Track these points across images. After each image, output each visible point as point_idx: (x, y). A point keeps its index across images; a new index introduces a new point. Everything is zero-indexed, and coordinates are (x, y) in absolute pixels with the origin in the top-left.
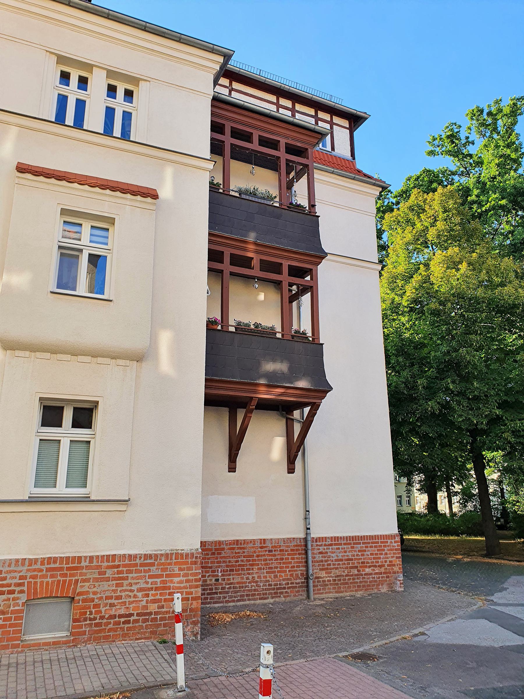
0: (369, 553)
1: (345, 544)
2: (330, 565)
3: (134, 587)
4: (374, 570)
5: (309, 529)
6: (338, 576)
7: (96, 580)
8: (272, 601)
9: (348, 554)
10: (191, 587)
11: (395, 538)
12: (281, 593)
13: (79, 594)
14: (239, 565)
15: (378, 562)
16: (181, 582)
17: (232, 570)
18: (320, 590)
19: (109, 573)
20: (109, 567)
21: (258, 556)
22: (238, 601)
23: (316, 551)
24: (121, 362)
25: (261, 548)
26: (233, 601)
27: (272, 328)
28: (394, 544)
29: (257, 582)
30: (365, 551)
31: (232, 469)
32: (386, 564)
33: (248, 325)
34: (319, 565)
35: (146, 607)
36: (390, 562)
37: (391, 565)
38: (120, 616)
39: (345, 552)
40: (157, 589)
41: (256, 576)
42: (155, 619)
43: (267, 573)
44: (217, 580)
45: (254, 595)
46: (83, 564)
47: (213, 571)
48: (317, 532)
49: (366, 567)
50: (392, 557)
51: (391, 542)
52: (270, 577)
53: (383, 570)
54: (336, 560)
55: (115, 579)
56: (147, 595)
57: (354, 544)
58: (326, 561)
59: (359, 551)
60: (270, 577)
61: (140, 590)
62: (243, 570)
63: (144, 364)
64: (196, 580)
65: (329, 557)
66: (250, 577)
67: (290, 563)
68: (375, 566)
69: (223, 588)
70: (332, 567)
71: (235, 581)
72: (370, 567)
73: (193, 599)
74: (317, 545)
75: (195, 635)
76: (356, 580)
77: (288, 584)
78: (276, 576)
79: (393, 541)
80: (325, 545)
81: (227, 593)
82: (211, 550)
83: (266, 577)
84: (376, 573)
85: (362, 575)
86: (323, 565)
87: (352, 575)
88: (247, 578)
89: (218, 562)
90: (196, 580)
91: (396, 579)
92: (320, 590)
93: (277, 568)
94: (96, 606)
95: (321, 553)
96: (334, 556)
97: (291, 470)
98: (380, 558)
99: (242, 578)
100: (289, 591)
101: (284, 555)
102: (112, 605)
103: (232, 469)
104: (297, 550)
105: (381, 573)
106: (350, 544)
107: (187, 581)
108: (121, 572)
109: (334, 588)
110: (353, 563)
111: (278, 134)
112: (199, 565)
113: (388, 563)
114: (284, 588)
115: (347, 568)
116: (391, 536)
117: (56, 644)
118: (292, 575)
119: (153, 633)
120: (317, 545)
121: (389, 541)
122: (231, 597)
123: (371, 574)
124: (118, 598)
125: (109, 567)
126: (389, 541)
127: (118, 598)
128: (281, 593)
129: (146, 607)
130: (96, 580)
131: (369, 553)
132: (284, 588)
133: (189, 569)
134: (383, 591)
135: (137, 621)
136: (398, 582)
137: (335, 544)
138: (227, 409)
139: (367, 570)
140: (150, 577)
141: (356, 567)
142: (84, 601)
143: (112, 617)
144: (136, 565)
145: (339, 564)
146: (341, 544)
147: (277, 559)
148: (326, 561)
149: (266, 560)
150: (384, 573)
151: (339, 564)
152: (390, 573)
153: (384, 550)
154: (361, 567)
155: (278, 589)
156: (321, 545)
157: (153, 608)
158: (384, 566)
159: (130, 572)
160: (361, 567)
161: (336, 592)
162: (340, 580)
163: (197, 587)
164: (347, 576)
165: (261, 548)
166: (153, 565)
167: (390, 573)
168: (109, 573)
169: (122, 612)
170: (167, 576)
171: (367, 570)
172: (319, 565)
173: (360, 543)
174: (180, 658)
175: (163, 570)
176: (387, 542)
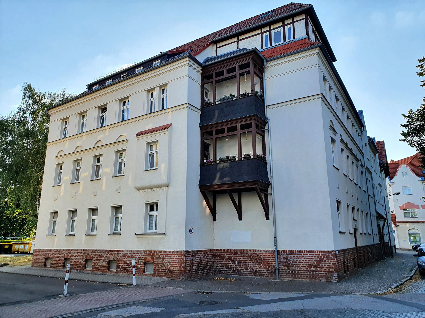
0: (313, 260)
1: (298, 254)
2: (289, 264)
3: (167, 261)
4: (316, 269)
5: (275, 246)
6: (294, 270)
7: (158, 258)
8: (260, 277)
9: (300, 259)
10: (182, 263)
11: (331, 253)
12: (264, 275)
13: (155, 262)
14: (245, 260)
15: (319, 265)
16: (179, 261)
17: (241, 262)
18: (284, 275)
19: (161, 256)
20: (161, 254)
21: (253, 257)
22: (245, 275)
23: (281, 257)
24: (163, 188)
25: (254, 253)
26: (243, 275)
27: (234, 157)
28: (331, 256)
29: (252, 268)
30: (311, 259)
31: (240, 219)
32: (325, 267)
33: (224, 159)
34: (283, 264)
35: (170, 268)
36: (327, 266)
37: (328, 267)
38: (164, 270)
39: (298, 258)
40: (173, 262)
41: (252, 266)
42: (172, 272)
43: (257, 265)
44: (236, 266)
45: (251, 274)
46: (155, 253)
47: (234, 262)
48: (281, 248)
49: (312, 267)
50: (329, 263)
51: (329, 255)
52: (259, 267)
53: (323, 270)
54: (293, 262)
55: (162, 258)
56: (170, 264)
57: (304, 254)
58: (287, 262)
59: (307, 258)
60: (259, 267)
61: (168, 262)
62: (246, 262)
63: (169, 187)
64: (183, 261)
65: (289, 260)
66: (249, 266)
67: (268, 261)
68: (318, 267)
69: (238, 269)
70: (290, 265)
71: (243, 267)
72: (314, 267)
73: (182, 267)
74: (282, 254)
75: (183, 279)
76: (305, 273)
77: (267, 271)
78: (261, 267)
79: (330, 254)
80: (286, 254)
81: (240, 271)
82: (233, 253)
83: (256, 267)
84: (317, 271)
85: (309, 271)
86: (286, 264)
87: (303, 271)
88: (248, 266)
89: (236, 258)
90: (183, 261)
91: (332, 275)
92: (284, 275)
93: (261, 263)
94: (158, 266)
95: (284, 258)
96: (292, 260)
97: (267, 218)
98: (321, 263)
99: (246, 266)
100: (268, 274)
101: (265, 257)
102: (162, 266)
103: (240, 219)
104: (271, 256)
105: (321, 271)
106: (301, 254)
107: (181, 261)
108: (163, 256)
109: (292, 276)
110: (303, 265)
111: (232, 64)
112: (184, 256)
113: (326, 266)
114: (266, 273)
115: (299, 266)
116: (329, 251)
117: (150, 275)
118: (269, 267)
119: (172, 276)
120: (282, 254)
121: (327, 254)
122: (241, 273)
123: (315, 271)
124: (163, 264)
125: (161, 254)
126: (327, 254)
127: (163, 264)
128: (264, 275)
129: (170, 268)
130: (158, 258)
131: (313, 260)
132: (266, 273)
133: (181, 257)
134: (322, 281)
135: (167, 272)
136: (334, 278)
137: (292, 254)
138: (227, 194)
139: (312, 269)
140: (171, 258)
141: (305, 267)
142: (156, 264)
143: (162, 270)
144: (167, 254)
145: (294, 264)
146: (296, 254)
147: (261, 259)
148: (287, 262)
149: (256, 259)
150: (323, 271)
151: (294, 264)
152: (328, 272)
153: (324, 259)
154: (308, 267)
155: (262, 272)
156: (284, 254)
157: (172, 268)
158: (323, 267)
159: (166, 256)
160: (308, 267)
161: (293, 278)
162: (295, 272)
163: (183, 263)
164: (299, 270)
165: (254, 253)
166: (171, 254)
167: (328, 272)
168: (161, 256)
169: (164, 268)
170: (175, 259)
171: (312, 269)
172: (283, 264)
173: (307, 255)
174: (134, 277)
175: (174, 257)
176: (326, 255)
